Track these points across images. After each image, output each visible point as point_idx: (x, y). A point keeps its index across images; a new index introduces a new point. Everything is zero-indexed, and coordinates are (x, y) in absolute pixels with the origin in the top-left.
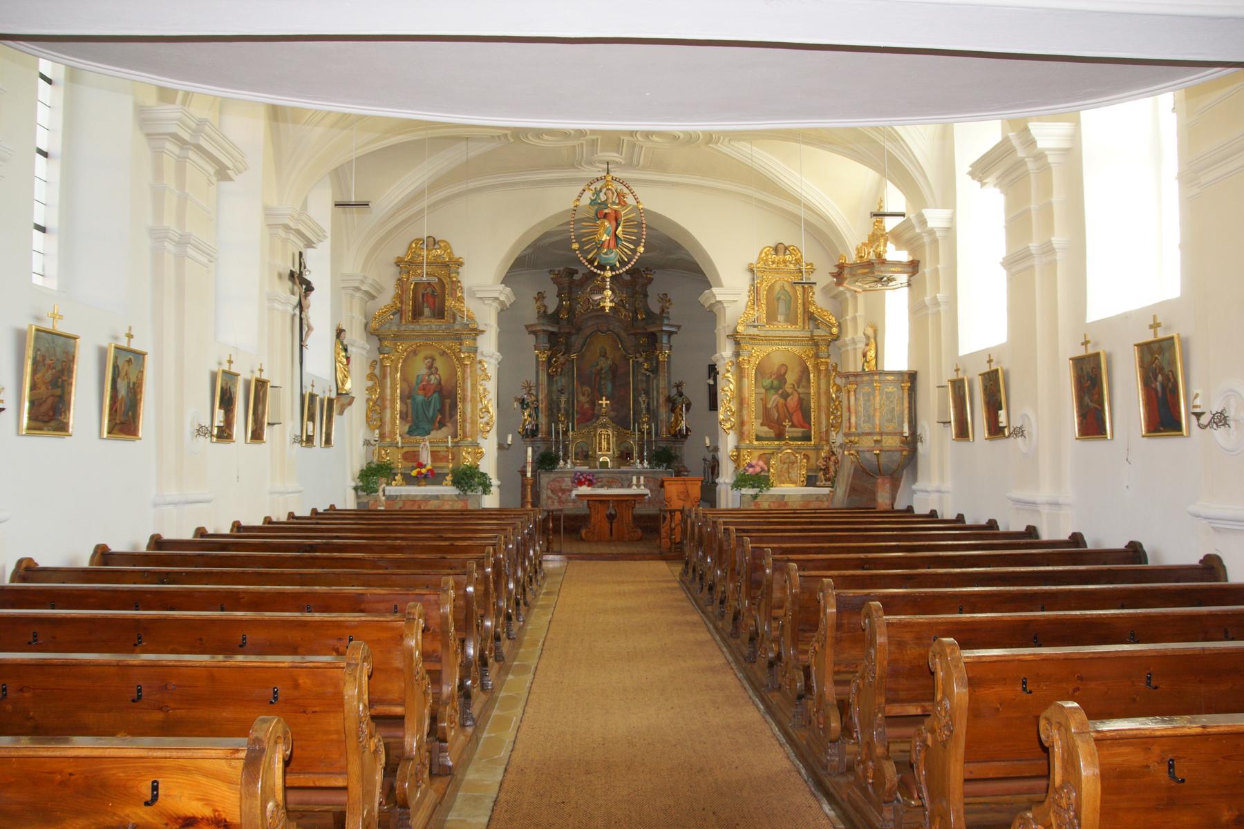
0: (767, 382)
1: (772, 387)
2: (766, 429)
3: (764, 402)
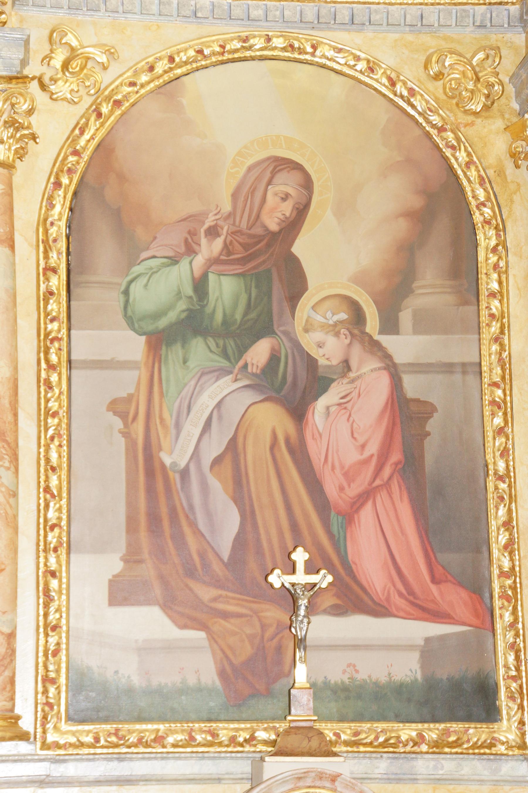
0: (162, 288)
1: (193, 323)
2: (149, 622)
3: (141, 426)
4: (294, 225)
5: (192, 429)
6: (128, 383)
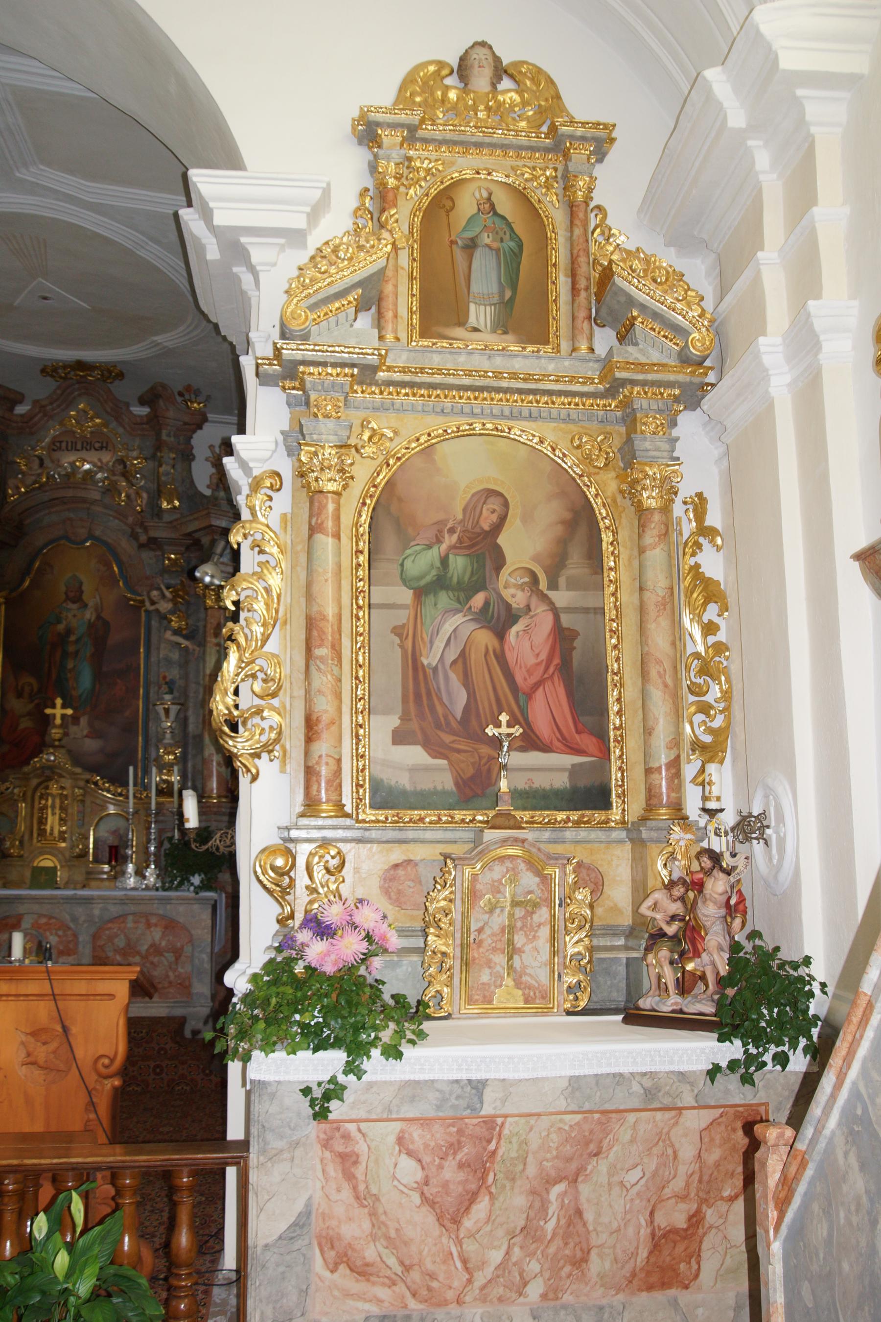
0: (422, 562)
2: (415, 754)
4: (498, 527)
5: (440, 644)
6: (402, 617)
